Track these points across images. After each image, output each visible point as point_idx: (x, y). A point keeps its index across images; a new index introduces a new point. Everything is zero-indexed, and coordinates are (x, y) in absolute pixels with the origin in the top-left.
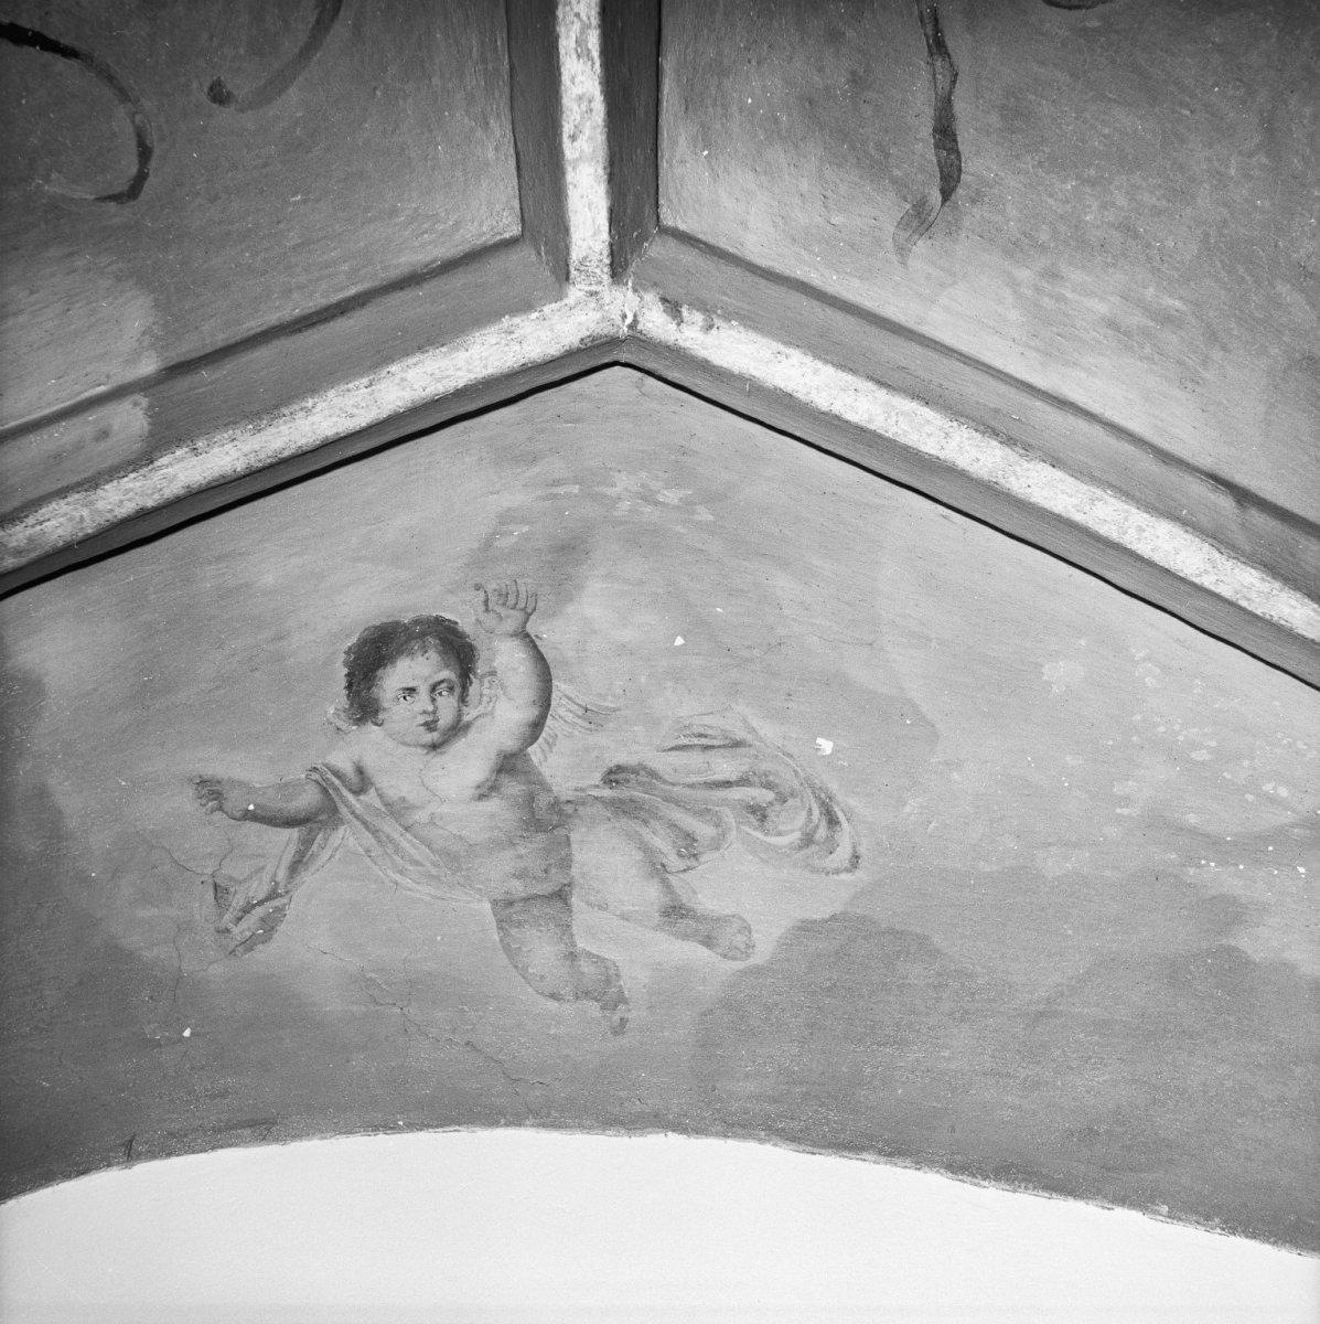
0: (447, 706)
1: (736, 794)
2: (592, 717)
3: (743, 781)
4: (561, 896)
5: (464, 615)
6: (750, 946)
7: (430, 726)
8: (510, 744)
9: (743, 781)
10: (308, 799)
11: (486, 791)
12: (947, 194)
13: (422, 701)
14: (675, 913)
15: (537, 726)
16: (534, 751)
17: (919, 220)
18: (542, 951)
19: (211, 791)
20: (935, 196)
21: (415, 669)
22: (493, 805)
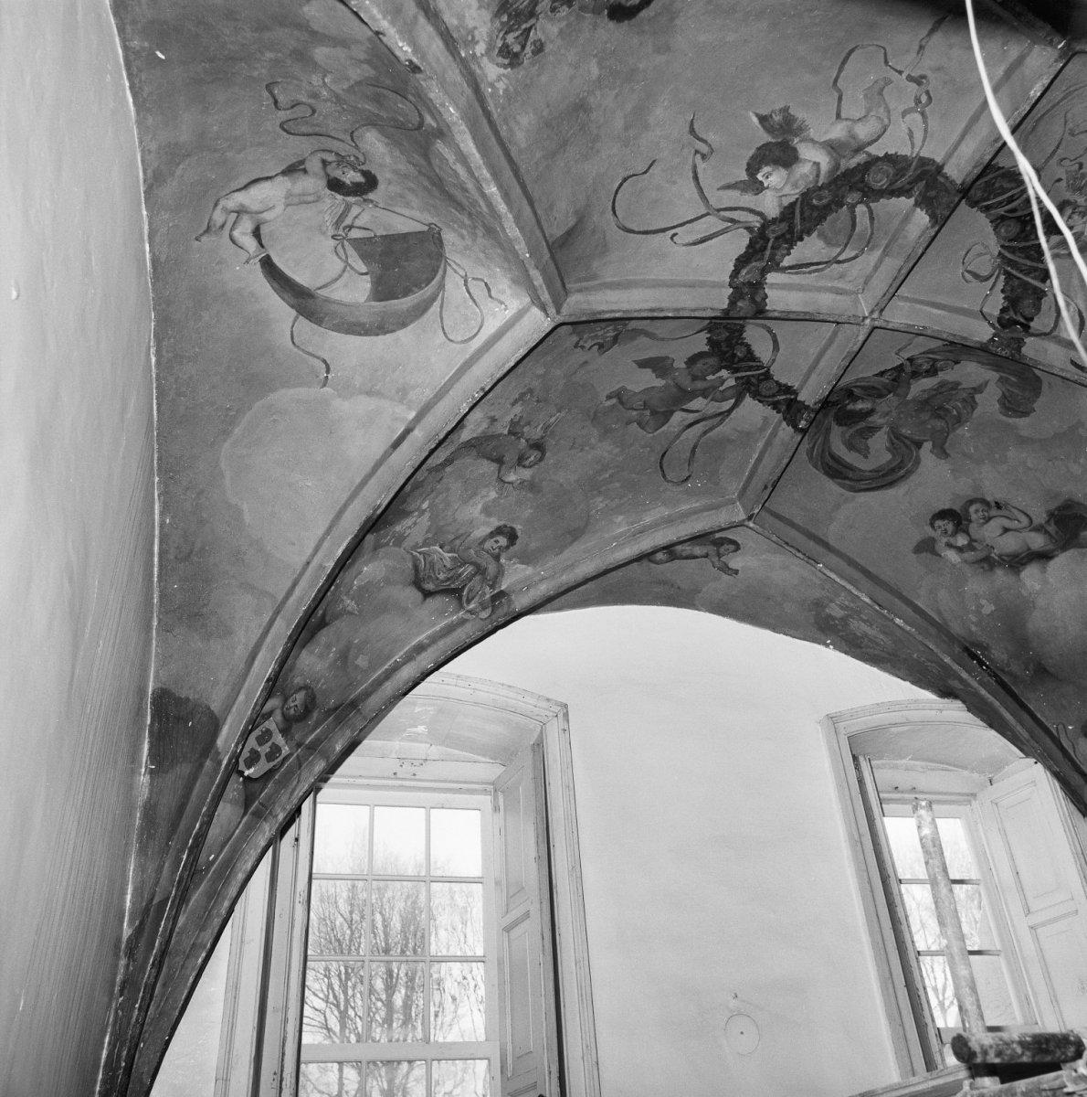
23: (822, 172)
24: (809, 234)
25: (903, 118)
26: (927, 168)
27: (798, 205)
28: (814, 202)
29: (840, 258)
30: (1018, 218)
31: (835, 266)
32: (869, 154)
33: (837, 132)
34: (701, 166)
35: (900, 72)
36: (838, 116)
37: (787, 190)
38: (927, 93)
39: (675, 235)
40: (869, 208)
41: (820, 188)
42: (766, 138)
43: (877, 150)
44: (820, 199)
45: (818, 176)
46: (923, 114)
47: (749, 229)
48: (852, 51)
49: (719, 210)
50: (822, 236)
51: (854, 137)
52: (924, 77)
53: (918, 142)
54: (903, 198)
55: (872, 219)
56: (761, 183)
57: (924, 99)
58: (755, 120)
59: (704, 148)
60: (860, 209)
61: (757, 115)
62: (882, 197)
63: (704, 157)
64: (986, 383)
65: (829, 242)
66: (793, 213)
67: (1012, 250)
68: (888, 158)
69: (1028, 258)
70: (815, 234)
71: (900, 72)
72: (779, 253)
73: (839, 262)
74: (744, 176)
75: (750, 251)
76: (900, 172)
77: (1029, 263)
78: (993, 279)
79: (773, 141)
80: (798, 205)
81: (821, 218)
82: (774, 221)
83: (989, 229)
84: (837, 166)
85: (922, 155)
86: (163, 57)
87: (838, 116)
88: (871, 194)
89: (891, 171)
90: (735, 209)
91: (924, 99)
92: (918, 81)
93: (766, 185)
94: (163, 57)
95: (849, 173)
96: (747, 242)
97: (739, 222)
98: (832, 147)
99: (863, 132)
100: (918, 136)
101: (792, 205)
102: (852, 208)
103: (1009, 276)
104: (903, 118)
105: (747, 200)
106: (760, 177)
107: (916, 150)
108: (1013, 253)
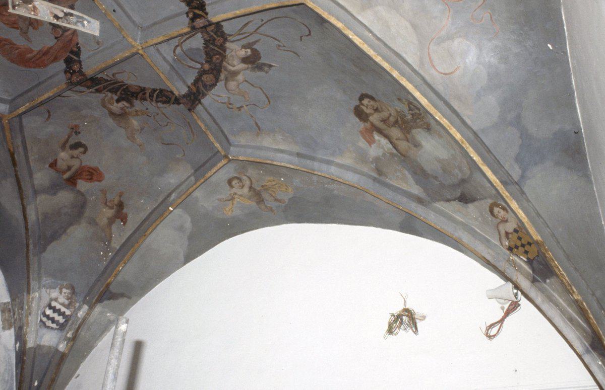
0: (241, 184)
1: (276, 186)
2: (257, 181)
3: (276, 184)
4: (263, 200)
5: (237, 175)
6: (285, 202)
7: (240, 186)
8: (250, 186)
9: (276, 184)
10: (230, 198)
11: (250, 191)
12: (260, 130)
13: (238, 184)
14: (276, 200)
15: (251, 183)
16: (253, 186)
17: (258, 135)
18: (263, 207)
19: (220, 200)
20: (259, 131)
21: (234, 182)
22: (251, 192)
23: (228, 66)
24: (205, 48)
25: (228, 97)
26: (201, 95)
27: (222, 52)
28: (217, 56)
29: (179, 48)
30: (138, 93)
31: (177, 44)
32: (221, 80)
33: (240, 77)
34: (277, 43)
35: (247, 106)
36: (246, 81)
37: (233, 53)
38: (232, 108)
39: (262, 20)
40: (197, 69)
41: (222, 61)
42: (262, 61)
43: (220, 84)
44: (217, 59)
45: (229, 64)
46: (225, 103)
47: (230, 35)
48: (269, 101)
49: (251, 34)
50: (198, 49)
51: (233, 80)
52: (240, 110)
53: (213, 96)
54: (193, 81)
55: (190, 67)
56: (246, 49)
57: (230, 106)
58: (274, 65)
59: (282, 48)
60: (199, 66)
61: (274, 66)
62: (199, 75)
63: (279, 46)
64: (29, 40)
65: (191, 49)
66: (222, 50)
67: (121, 86)
68: (214, 85)
69: (113, 88)
70: (202, 48)
71: (247, 106)
72: (206, 36)
73: (177, 46)
74: (255, 47)
75: (220, 31)
76: (205, 86)
77: (109, 88)
78: (111, 77)
79: (258, 62)
80: (222, 52)
81: (207, 54)
82: (224, 42)
83: (142, 85)
84: (226, 70)
85: (208, 96)
86: (551, 48)
87: (246, 81)
88: (202, 73)
89: (208, 83)
90: (244, 38)
91: (230, 106)
92: (239, 108)
93: (243, 50)
94: (551, 48)
95: (219, 72)
96: (226, 32)
97: (238, 35)
98: (235, 74)
99: (232, 85)
100: (217, 98)
101: (225, 51)
102: (202, 64)
103: (107, 81)
104: (228, 97)
105: (244, 42)
106: (249, 50)
107: (211, 95)
108: (121, 85)
